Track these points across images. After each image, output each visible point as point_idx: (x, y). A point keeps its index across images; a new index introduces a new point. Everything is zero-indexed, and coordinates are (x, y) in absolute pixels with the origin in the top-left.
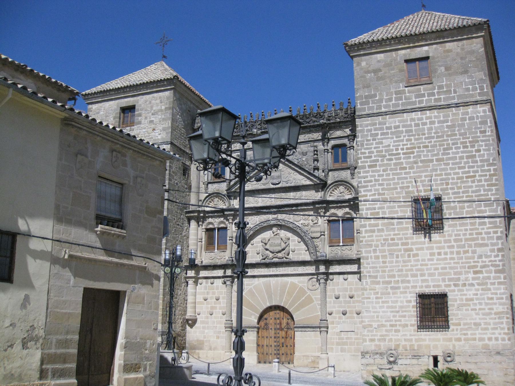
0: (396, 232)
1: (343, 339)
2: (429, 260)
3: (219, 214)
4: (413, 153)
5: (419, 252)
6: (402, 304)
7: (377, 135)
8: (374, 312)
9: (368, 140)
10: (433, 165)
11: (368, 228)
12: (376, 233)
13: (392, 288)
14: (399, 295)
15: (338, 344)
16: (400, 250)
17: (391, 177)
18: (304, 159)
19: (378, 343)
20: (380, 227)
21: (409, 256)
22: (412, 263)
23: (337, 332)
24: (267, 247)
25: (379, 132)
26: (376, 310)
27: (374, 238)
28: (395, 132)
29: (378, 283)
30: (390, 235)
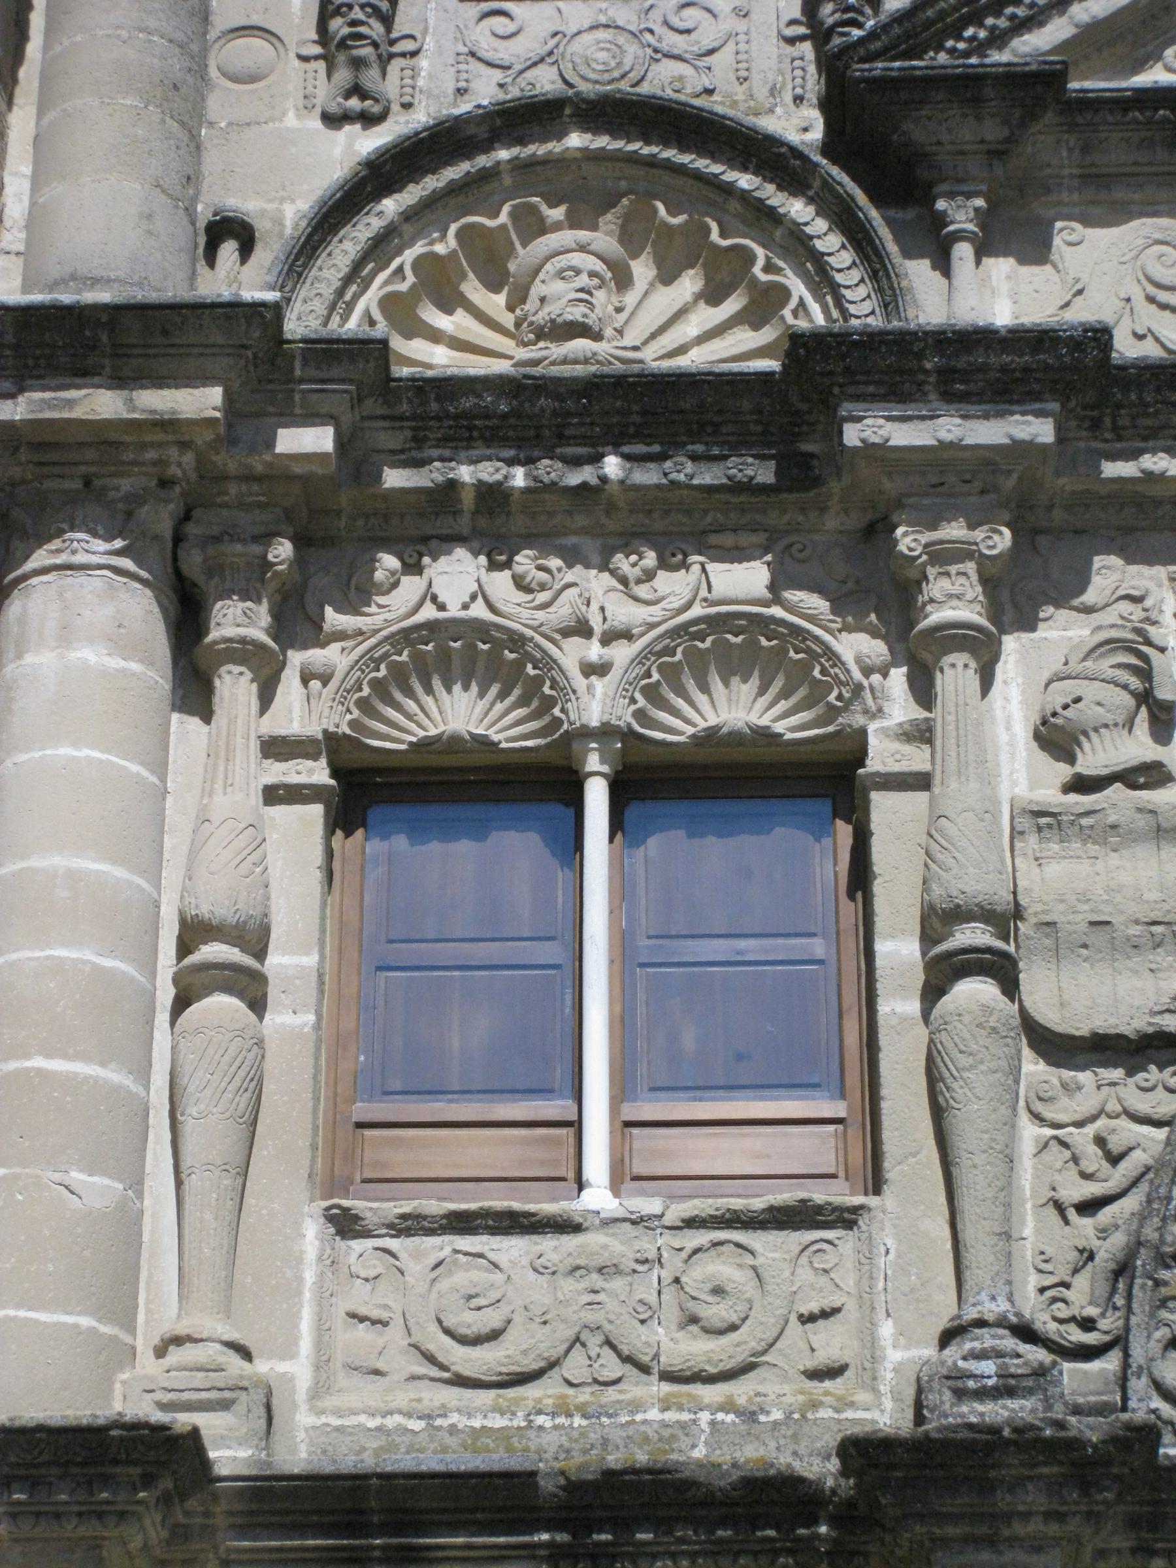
3: (686, 471)
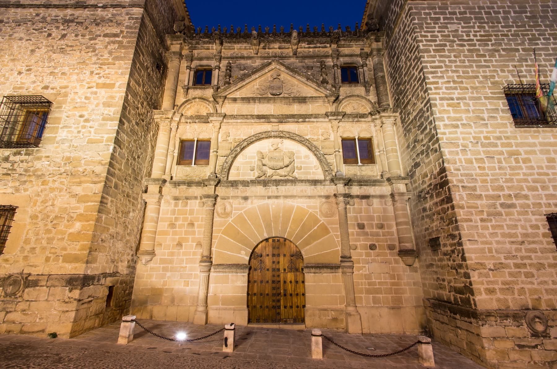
0: (490, 129)
1: (374, 284)
2: (548, 167)
4: (491, 41)
5: (531, 157)
6: (524, 231)
7: (439, 19)
8: (483, 243)
9: (427, 23)
10: (519, 55)
11: (447, 122)
12: (461, 129)
13: (502, 205)
14: (516, 216)
15: (368, 292)
16: (502, 153)
17: (467, 64)
18: (309, 73)
19: (502, 297)
20: (465, 122)
21: (517, 161)
22: (524, 171)
23: (365, 275)
24: (264, 162)
25: (442, 17)
26: (485, 239)
27: (459, 135)
28: (461, 17)
29: (480, 197)
30: (482, 132)
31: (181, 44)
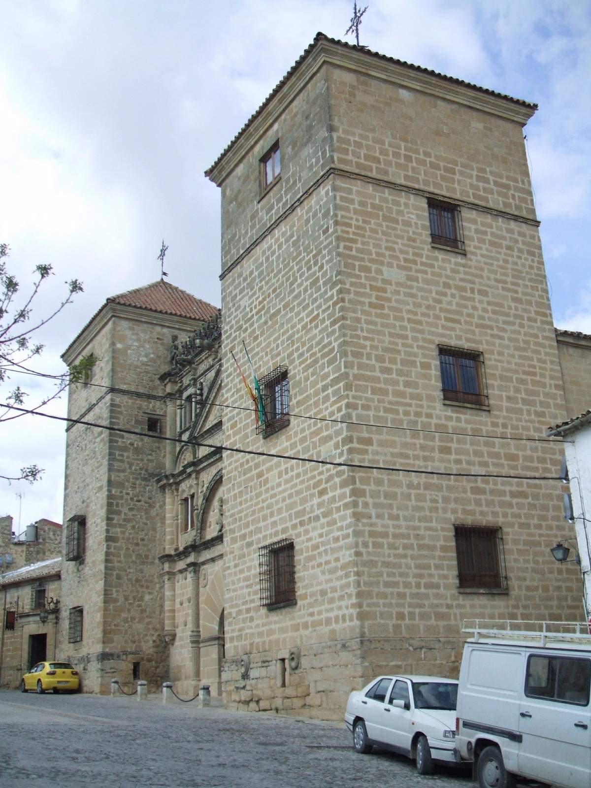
31: (170, 381)
